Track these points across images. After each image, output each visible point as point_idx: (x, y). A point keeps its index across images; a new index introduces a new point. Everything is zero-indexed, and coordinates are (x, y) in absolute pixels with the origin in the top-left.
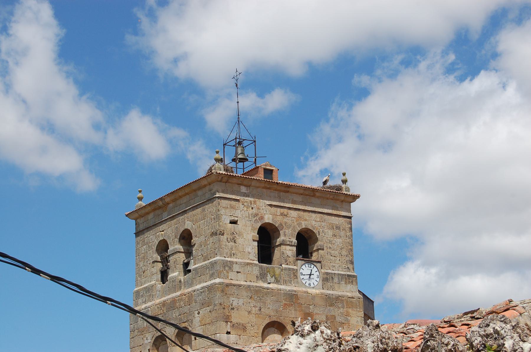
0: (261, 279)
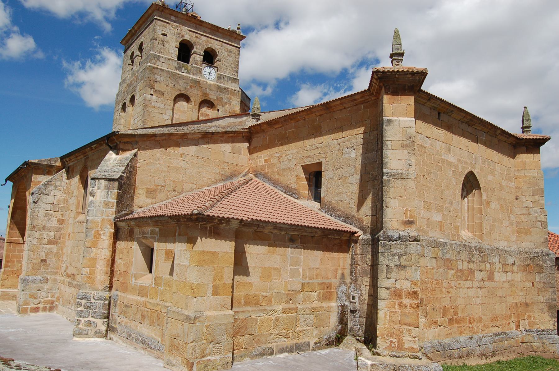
0: (178, 69)
